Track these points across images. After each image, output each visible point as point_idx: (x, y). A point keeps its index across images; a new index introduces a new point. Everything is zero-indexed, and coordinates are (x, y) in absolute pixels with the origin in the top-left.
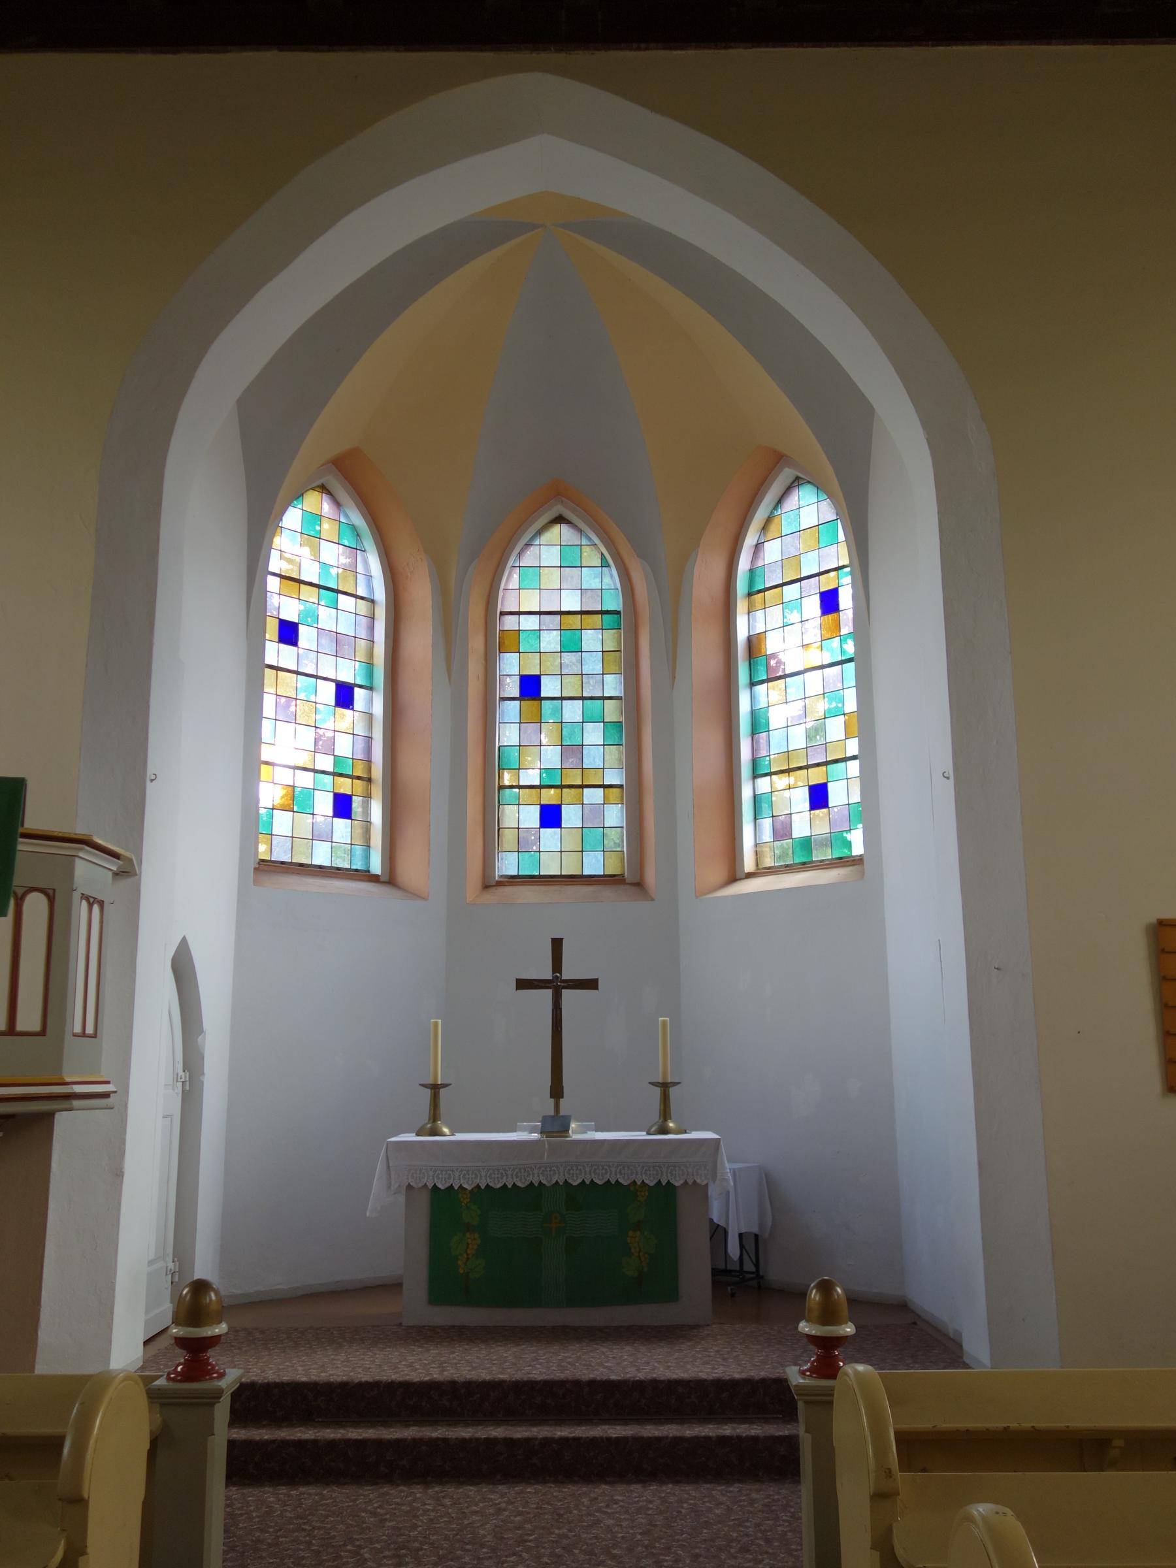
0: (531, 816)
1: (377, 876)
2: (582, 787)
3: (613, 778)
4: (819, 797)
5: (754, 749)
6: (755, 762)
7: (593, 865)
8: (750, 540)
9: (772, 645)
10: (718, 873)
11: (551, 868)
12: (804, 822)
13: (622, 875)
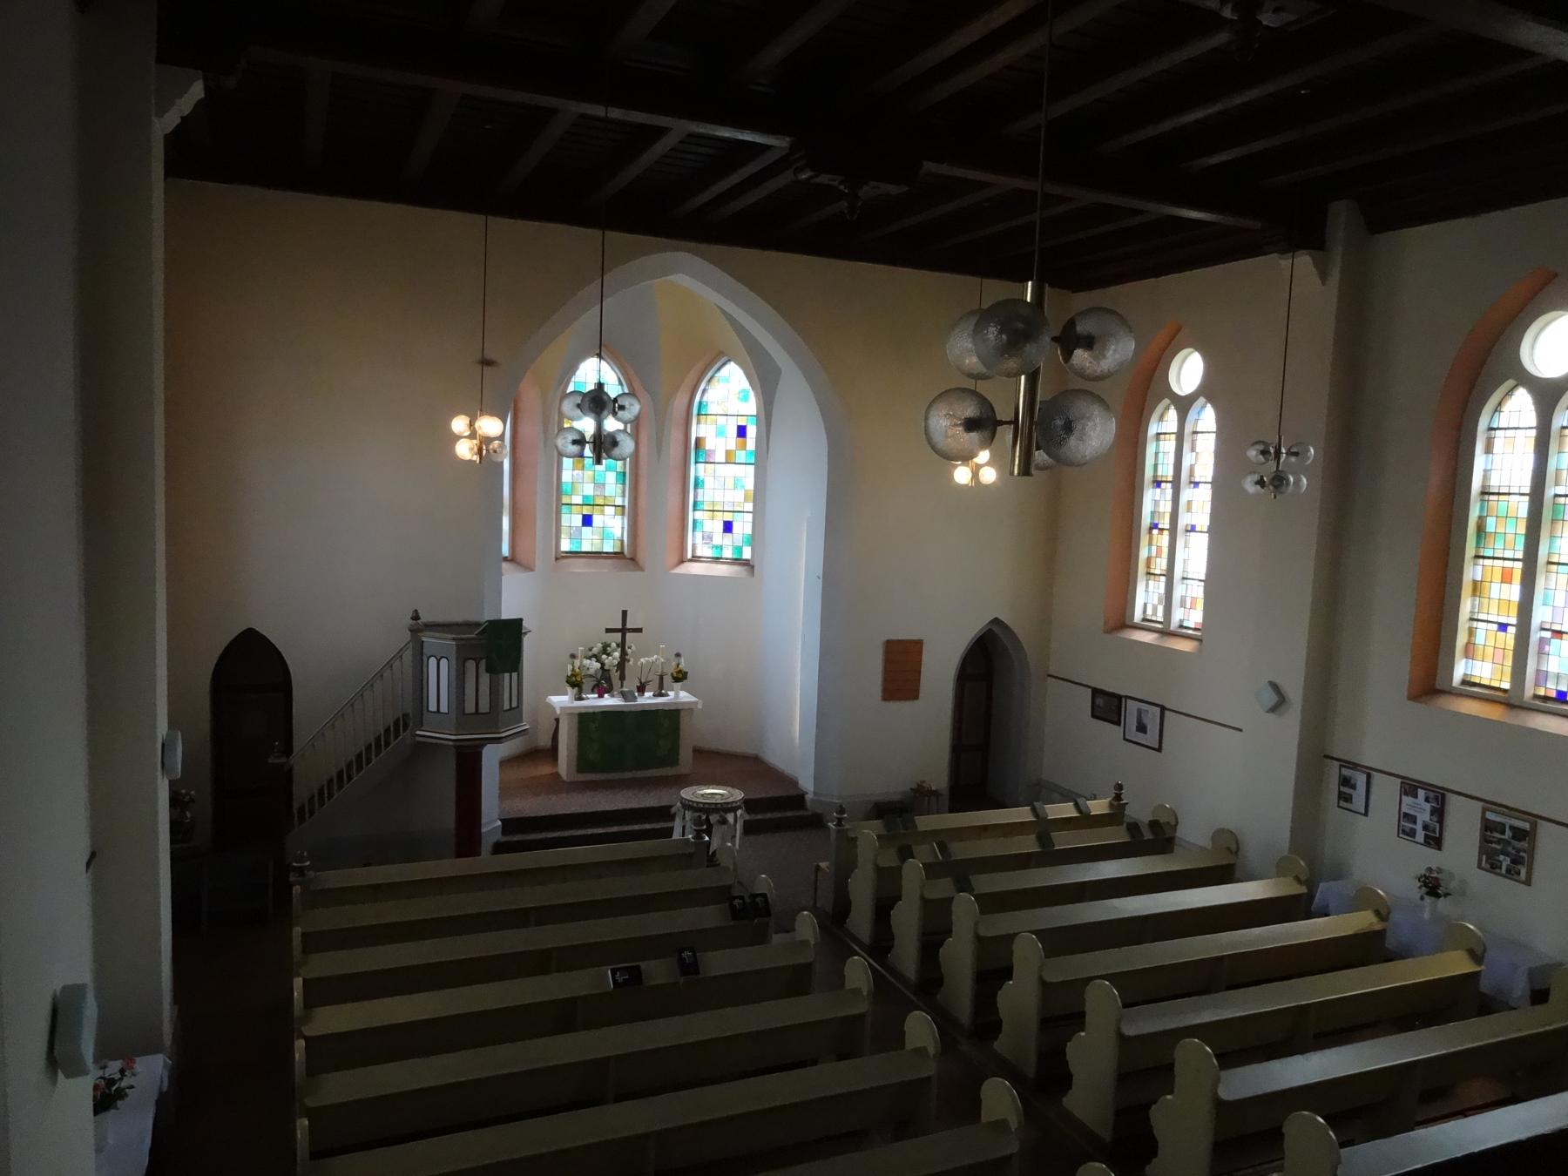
0: (577, 520)
1: (506, 557)
2: (603, 505)
3: (619, 501)
4: (728, 527)
5: (696, 496)
6: (695, 503)
7: (609, 547)
8: (702, 387)
9: (709, 445)
10: (674, 558)
11: (586, 547)
12: (719, 537)
13: (622, 553)
